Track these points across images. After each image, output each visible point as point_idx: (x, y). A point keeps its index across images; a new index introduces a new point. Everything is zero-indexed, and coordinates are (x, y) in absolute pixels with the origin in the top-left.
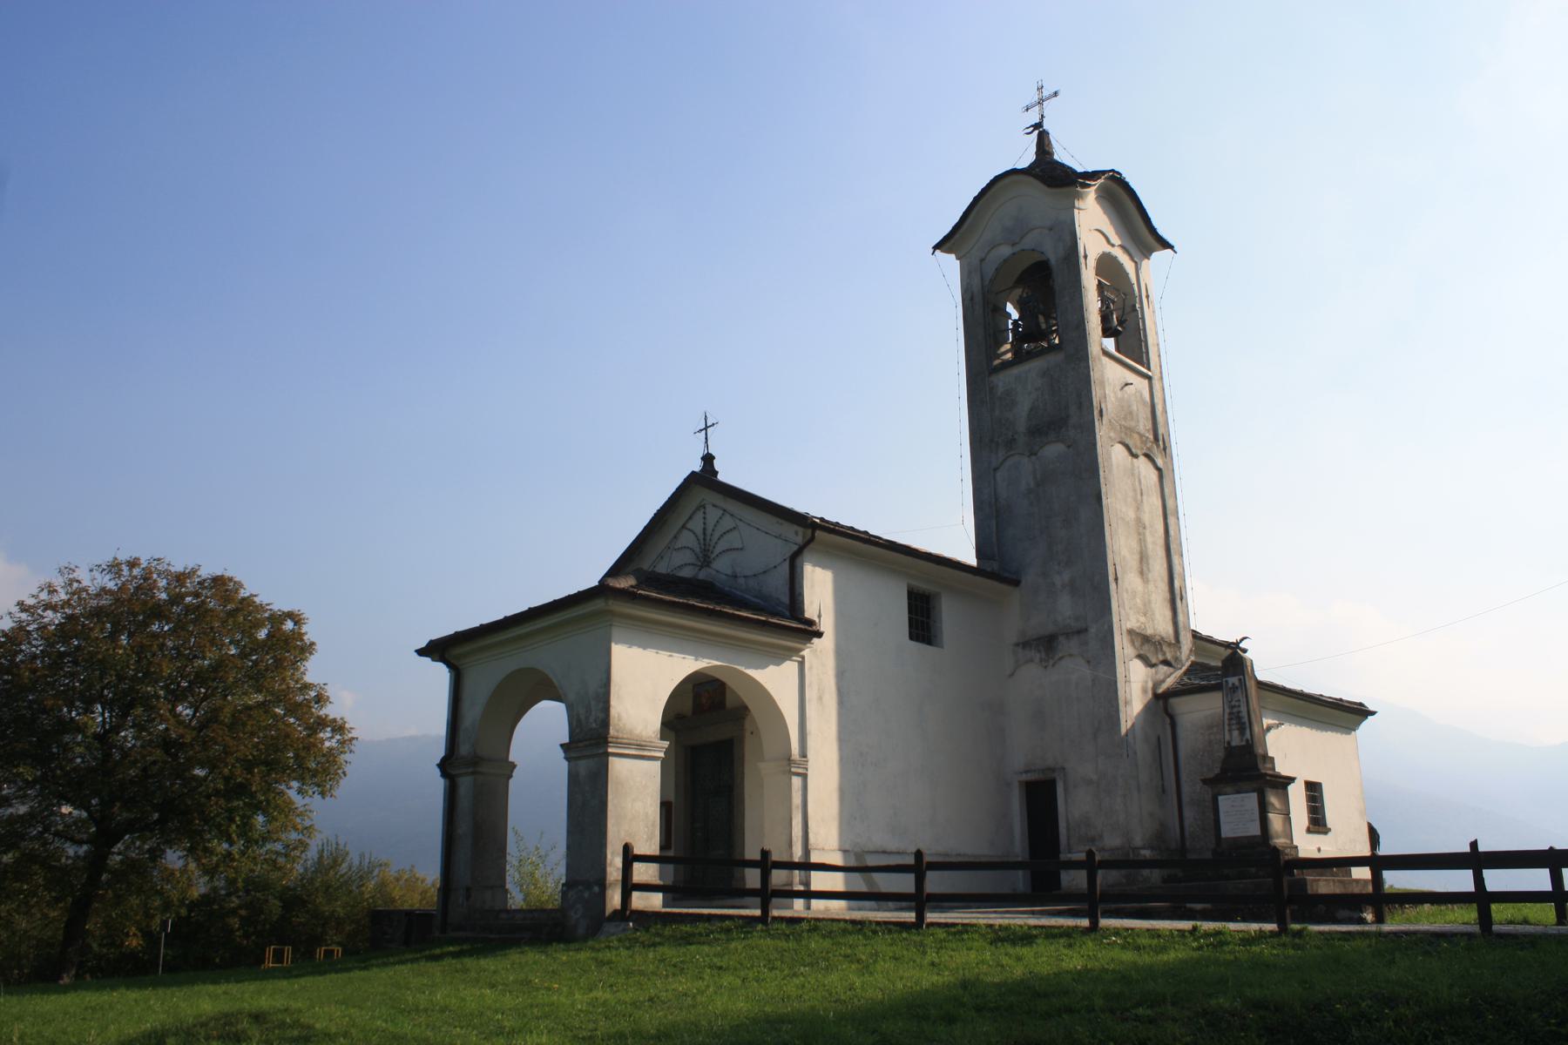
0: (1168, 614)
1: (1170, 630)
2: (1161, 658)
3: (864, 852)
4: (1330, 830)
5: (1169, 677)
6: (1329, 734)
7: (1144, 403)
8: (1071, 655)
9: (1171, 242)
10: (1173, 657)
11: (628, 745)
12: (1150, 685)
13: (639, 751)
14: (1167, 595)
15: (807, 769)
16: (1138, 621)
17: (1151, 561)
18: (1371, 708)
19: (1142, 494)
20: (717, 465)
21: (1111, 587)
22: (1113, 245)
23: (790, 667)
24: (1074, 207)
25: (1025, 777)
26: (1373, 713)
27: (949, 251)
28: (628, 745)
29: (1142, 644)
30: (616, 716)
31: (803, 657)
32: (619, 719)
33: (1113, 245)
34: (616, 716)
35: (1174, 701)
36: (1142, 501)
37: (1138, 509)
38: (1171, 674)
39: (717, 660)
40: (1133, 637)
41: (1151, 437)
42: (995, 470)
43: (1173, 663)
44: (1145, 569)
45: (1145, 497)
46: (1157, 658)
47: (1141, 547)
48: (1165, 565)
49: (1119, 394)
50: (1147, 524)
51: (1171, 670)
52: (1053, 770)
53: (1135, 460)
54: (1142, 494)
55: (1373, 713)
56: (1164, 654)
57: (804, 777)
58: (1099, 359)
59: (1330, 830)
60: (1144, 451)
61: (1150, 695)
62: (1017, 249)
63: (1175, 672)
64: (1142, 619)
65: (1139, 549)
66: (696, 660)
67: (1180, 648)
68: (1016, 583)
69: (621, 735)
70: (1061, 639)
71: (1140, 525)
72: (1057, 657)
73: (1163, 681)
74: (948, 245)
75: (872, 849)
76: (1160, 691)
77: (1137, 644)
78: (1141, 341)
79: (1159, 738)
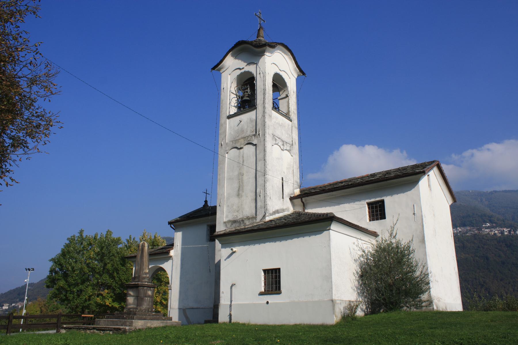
22: (243, 68)
33: (243, 68)
40: (227, 224)
47: (240, 184)
53: (241, 150)
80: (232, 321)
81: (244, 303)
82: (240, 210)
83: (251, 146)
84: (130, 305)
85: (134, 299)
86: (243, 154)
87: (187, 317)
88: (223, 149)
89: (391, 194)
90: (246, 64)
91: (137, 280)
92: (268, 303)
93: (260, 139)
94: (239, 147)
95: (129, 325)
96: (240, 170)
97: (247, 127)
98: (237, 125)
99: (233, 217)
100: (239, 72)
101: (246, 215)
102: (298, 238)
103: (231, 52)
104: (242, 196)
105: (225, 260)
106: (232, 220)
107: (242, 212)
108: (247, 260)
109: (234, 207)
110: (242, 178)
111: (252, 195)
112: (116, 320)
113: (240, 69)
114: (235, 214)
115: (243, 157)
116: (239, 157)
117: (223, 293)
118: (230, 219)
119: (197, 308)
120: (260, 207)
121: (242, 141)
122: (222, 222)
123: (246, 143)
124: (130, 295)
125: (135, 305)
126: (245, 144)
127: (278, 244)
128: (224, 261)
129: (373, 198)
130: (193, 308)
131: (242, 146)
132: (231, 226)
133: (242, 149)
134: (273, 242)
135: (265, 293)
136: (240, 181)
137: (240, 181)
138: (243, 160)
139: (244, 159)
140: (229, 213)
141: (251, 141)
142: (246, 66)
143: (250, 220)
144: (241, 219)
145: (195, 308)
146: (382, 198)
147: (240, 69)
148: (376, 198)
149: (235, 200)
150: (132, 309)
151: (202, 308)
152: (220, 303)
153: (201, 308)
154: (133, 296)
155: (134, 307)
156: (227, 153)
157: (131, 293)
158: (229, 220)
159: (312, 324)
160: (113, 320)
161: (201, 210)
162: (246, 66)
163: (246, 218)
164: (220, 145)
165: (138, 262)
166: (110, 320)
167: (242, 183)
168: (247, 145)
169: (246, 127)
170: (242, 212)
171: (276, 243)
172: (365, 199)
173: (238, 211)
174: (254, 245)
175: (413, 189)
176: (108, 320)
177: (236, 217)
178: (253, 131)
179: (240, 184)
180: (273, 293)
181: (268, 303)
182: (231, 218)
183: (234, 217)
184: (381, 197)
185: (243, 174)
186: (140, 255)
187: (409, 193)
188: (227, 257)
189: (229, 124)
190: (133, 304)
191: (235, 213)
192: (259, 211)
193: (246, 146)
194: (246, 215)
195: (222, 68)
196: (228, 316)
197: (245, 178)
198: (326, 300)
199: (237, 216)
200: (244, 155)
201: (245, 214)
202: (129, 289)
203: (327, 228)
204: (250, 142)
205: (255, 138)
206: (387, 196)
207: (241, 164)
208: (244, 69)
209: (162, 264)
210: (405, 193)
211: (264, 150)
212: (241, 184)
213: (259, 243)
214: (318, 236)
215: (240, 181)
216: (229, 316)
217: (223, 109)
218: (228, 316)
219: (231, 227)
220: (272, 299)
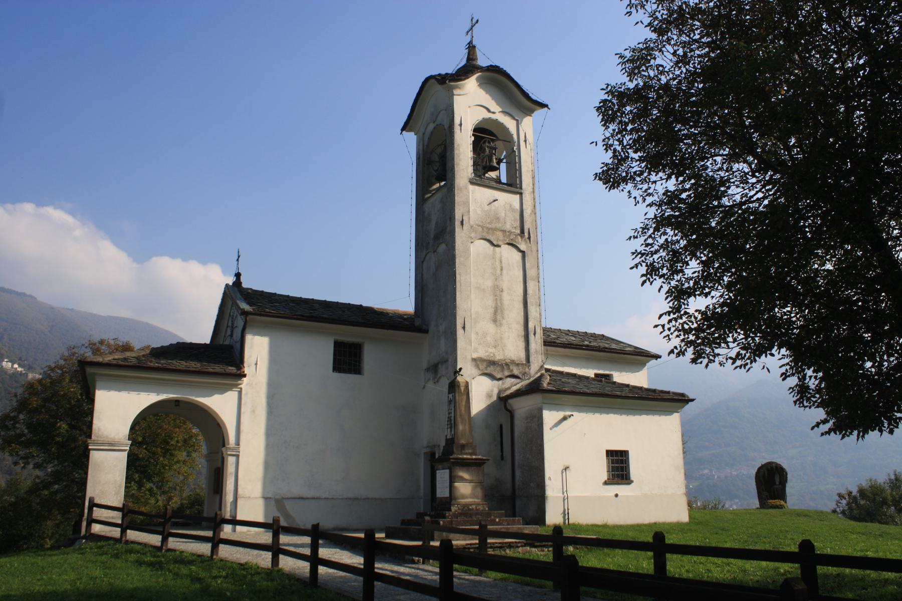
0: (522, 344)
1: (522, 355)
2: (507, 373)
3: (283, 498)
4: (632, 482)
6: (644, 417)
7: (512, 209)
8: (443, 376)
9: (546, 102)
10: (520, 373)
11: (103, 444)
12: (496, 392)
13: (112, 446)
14: (523, 333)
15: (239, 452)
16: (486, 352)
17: (506, 312)
18: (691, 397)
19: (502, 270)
20: (242, 279)
21: (458, 333)
22: (494, 113)
23: (232, 395)
24: (453, 95)
25: (426, 450)
26: (692, 400)
27: (410, 131)
28: (103, 444)
29: (488, 366)
30: (97, 429)
31: (241, 389)
32: (99, 429)
33: (494, 113)
34: (97, 429)
35: (511, 401)
36: (501, 274)
37: (497, 278)
38: (518, 383)
39: (174, 394)
40: (478, 362)
41: (518, 231)
42: (423, 262)
43: (521, 376)
44: (498, 317)
45: (504, 272)
46: (503, 374)
47: (496, 303)
49: (487, 208)
50: (505, 288)
51: (518, 380)
52: (434, 446)
53: (497, 249)
54: (502, 270)
55: (692, 400)
56: (512, 371)
57: (238, 456)
58: (466, 188)
59: (632, 482)
60: (507, 241)
61: (495, 398)
62: (436, 124)
65: (494, 306)
66: (158, 395)
67: (530, 366)
68: (426, 332)
69: (99, 439)
70: (440, 366)
71: (497, 291)
72: (438, 377)
73: (509, 388)
74: (408, 127)
75: (290, 495)
76: (501, 396)
77: (482, 366)
78: (516, 170)
79: (501, 426)
83: (514, 250)
84: (464, 497)
85: (474, 488)
88: (464, 231)
89: (621, 371)
90: (501, 110)
91: (470, 451)
92: (617, 495)
94: (495, 243)
98: (488, 203)
99: (487, 354)
100: (488, 115)
102: (647, 414)
104: (501, 325)
105: (551, 429)
106: (485, 358)
107: (503, 350)
109: (489, 339)
110: (501, 296)
111: (519, 329)
113: (489, 111)
114: (490, 350)
115: (501, 262)
116: (493, 258)
117: (550, 479)
119: (313, 498)
121: (500, 234)
122: (469, 358)
123: (507, 241)
124: (462, 480)
125: (478, 499)
126: (506, 242)
127: (624, 417)
130: (301, 498)
131: (500, 243)
132: (486, 368)
133: (499, 248)
136: (496, 299)
137: (496, 299)
139: (503, 265)
140: (479, 345)
141: (516, 242)
142: (499, 112)
144: (504, 362)
147: (489, 111)
149: (491, 328)
150: (474, 507)
151: (326, 499)
153: (324, 497)
154: (470, 482)
155: (475, 502)
156: (472, 242)
157: (466, 476)
162: (499, 112)
164: (457, 223)
165: (461, 415)
167: (501, 304)
168: (507, 246)
169: (503, 215)
170: (503, 350)
172: (593, 368)
173: (495, 347)
177: (492, 355)
179: (496, 303)
181: (617, 495)
182: (482, 353)
183: (488, 356)
184: (611, 370)
186: (464, 403)
190: (473, 495)
195: (460, 88)
197: (506, 297)
200: (503, 258)
206: (617, 371)
207: (499, 271)
209: (204, 396)
212: (499, 305)
213: (601, 413)
214: (668, 417)
215: (498, 300)
217: (460, 160)
219: (486, 370)
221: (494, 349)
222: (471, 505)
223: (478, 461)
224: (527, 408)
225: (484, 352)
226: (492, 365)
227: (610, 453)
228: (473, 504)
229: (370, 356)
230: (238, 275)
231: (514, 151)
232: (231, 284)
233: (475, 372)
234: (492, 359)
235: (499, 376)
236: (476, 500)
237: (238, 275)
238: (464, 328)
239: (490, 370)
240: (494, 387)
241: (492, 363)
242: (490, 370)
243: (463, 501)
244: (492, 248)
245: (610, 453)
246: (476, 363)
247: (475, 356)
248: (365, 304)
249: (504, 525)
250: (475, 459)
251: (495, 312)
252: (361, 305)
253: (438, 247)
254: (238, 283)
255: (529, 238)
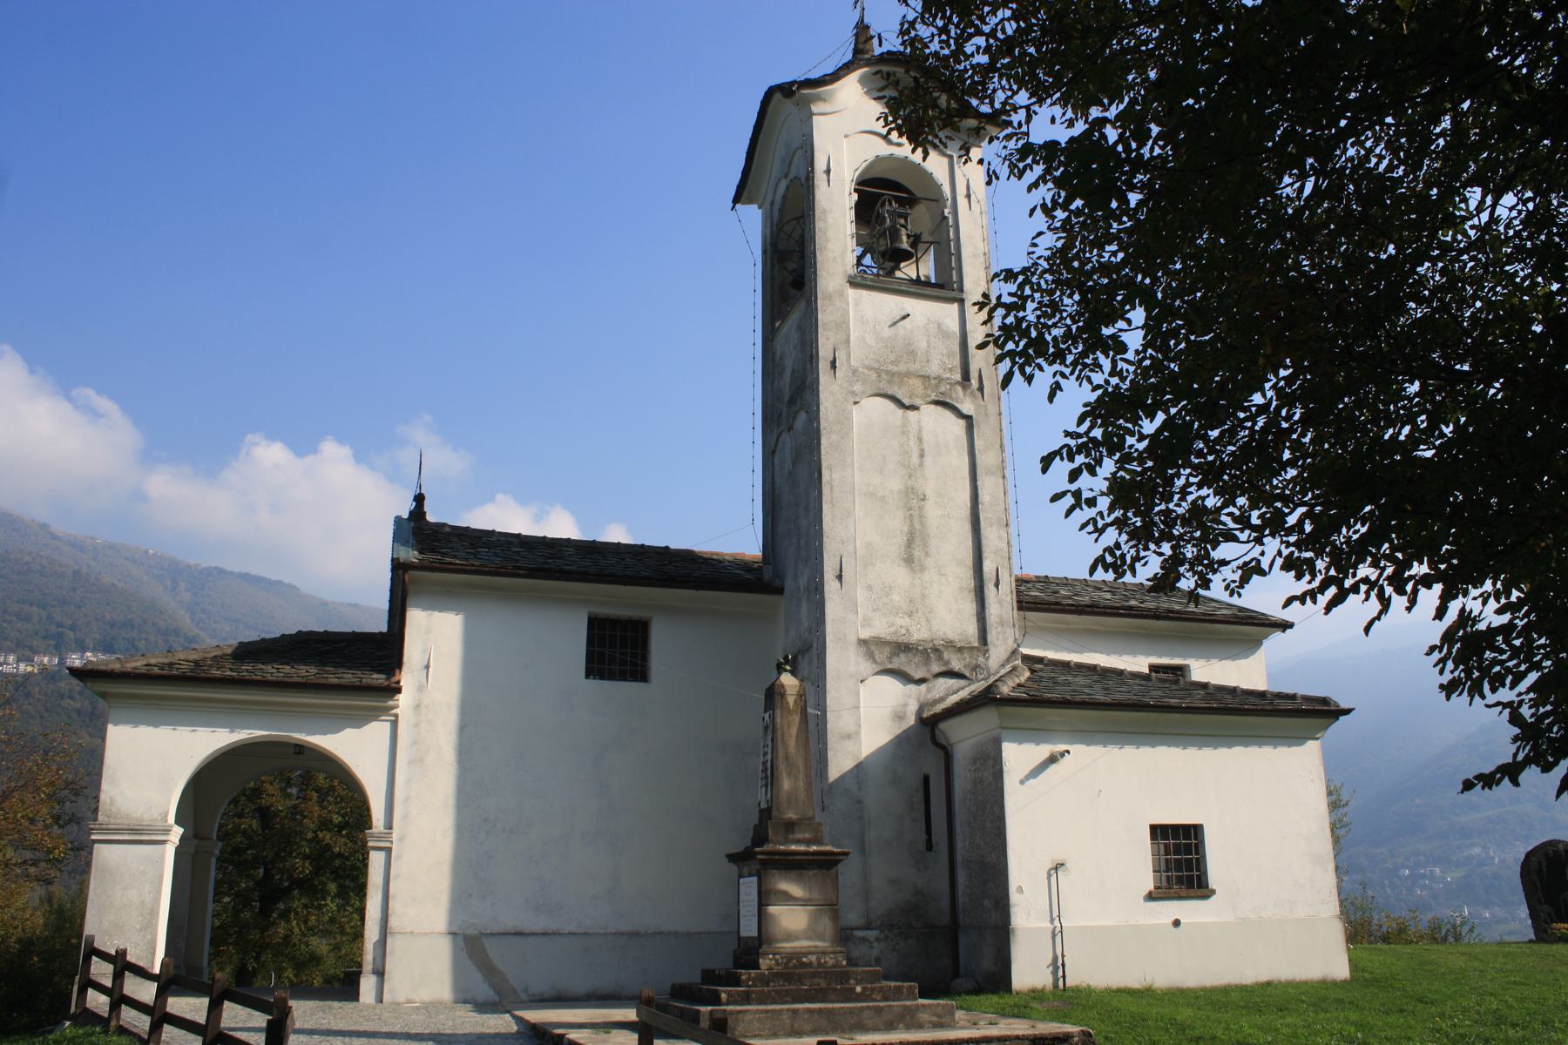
0: (970, 608)
1: (972, 629)
2: (936, 668)
3: (483, 934)
4: (1213, 892)
5: (952, 694)
6: (1238, 750)
7: (945, 335)
10: (965, 666)
11: (118, 831)
12: (913, 708)
13: (140, 835)
14: (971, 583)
15: (392, 842)
18: (1344, 705)
19: (922, 456)
20: (427, 508)
21: (826, 588)
23: (378, 730)
24: (812, 114)
26: (1347, 712)
27: (750, 201)
28: (118, 831)
30: (108, 800)
31: (396, 716)
32: (112, 800)
34: (108, 800)
35: (943, 726)
36: (921, 465)
38: (962, 689)
39: (262, 729)
40: (873, 648)
41: (958, 377)
43: (967, 674)
44: (917, 553)
45: (928, 459)
46: (929, 671)
47: (912, 525)
48: (970, 543)
49: (887, 332)
50: (929, 493)
51: (962, 682)
53: (910, 413)
54: (922, 456)
55: (1347, 712)
56: (947, 663)
57: (389, 850)
58: (842, 294)
59: (1213, 892)
60: (933, 397)
61: (911, 720)
63: (969, 685)
64: (906, 621)
65: (906, 529)
66: (232, 732)
67: (987, 651)
68: (779, 591)
69: (113, 821)
71: (913, 500)
74: (745, 194)
75: (496, 929)
76: (925, 716)
77: (882, 655)
79: (926, 779)
80: (1067, 985)
81: (1098, 924)
82: (920, 612)
83: (948, 415)
84: (790, 937)
85: (814, 919)
86: (920, 431)
87: (489, 970)
88: (838, 381)
89: (1208, 657)
91: (807, 835)
92: (1177, 923)
93: (985, 406)
94: (906, 401)
95: (930, 1022)
96: (910, 477)
97: (928, 347)
99: (892, 630)
101: (941, 633)
102: (1246, 745)
103: (866, 69)
104: (923, 569)
105: (1022, 782)
107: (928, 620)
108: (1101, 791)
109: (895, 597)
110: (921, 508)
112: (850, 1008)
115: (920, 440)
116: (904, 433)
117: (1020, 890)
118: (882, 636)
119: (544, 934)
120: (997, 620)
121: (917, 384)
122: (853, 639)
124: (787, 899)
125: (823, 940)
128: (1019, 785)
129: (1167, 655)
131: (917, 402)
132: (890, 659)
133: (915, 412)
134: (1178, 747)
135: (1168, 895)
138: (922, 450)
139: (926, 446)
140: (874, 610)
141: (951, 398)
143: (966, 655)
145: (533, 934)
146: (1186, 662)
148: (1173, 656)
149: (900, 576)
150: (813, 958)
152: (1010, 924)
153: (567, 931)
154: (804, 902)
155: (816, 947)
156: (856, 403)
157: (795, 890)
158: (875, 637)
159: (1298, 980)
160: (879, 1006)
161: (490, 545)
163: (942, 642)
164: (823, 366)
165: (787, 758)
166: (810, 1011)
167: (923, 525)
169: (924, 345)
170: (928, 620)
171: (1187, 750)
172: (1148, 654)
174: (1120, 748)
175: (1252, 657)
176: (795, 1012)
177: (903, 631)
178: (951, 370)
179: (912, 525)
180: (1193, 895)
181: (1177, 923)
182: (880, 627)
183: (895, 633)
184: (1185, 657)
185: (924, 496)
186: (794, 731)
187: (1243, 662)
188: (1027, 772)
189: (856, 305)
190: (811, 933)
191: (897, 618)
192: (994, 631)
193: (928, 406)
194: (944, 633)
195: (824, 100)
196: (1048, 967)
197: (932, 511)
198: (1323, 916)
199: (908, 630)
201: (937, 631)
202: (775, 871)
203: (1317, 733)
204: (948, 401)
205: (964, 395)
206: (1198, 657)
208: (900, 148)
209: (324, 733)
210: (1236, 661)
211: (1001, 446)
213: (1138, 744)
214: (1294, 749)
215: (915, 518)
216: (1051, 968)
217: (827, 241)
218: (1048, 967)
219: (891, 662)
220: (1188, 910)
221: (907, 619)
222: (806, 954)
223: (822, 858)
224: (973, 741)
225: (885, 625)
226: (904, 651)
227: (1158, 832)
228: (811, 953)
229: (664, 643)
230: (419, 499)
231: (945, 218)
232: (405, 515)
233: (866, 667)
234: (905, 640)
235: (918, 675)
236: (820, 944)
237: (419, 499)
238: (840, 577)
239: (899, 662)
240: (910, 697)
241: (903, 648)
242: (899, 662)
243: (788, 946)
244: (900, 412)
245: (1158, 832)
246: (868, 648)
247: (865, 634)
248: (676, 544)
249: (875, 1000)
250: (814, 853)
251: (910, 543)
252: (667, 548)
253: (794, 418)
254: (418, 512)
255: (981, 389)
